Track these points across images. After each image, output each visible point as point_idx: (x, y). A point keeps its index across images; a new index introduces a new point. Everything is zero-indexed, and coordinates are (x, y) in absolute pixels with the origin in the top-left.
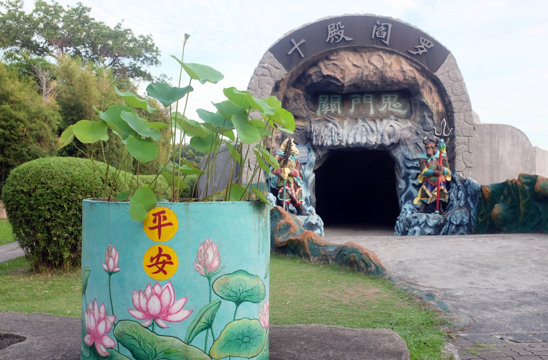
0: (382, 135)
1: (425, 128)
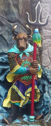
1: (10, 18)
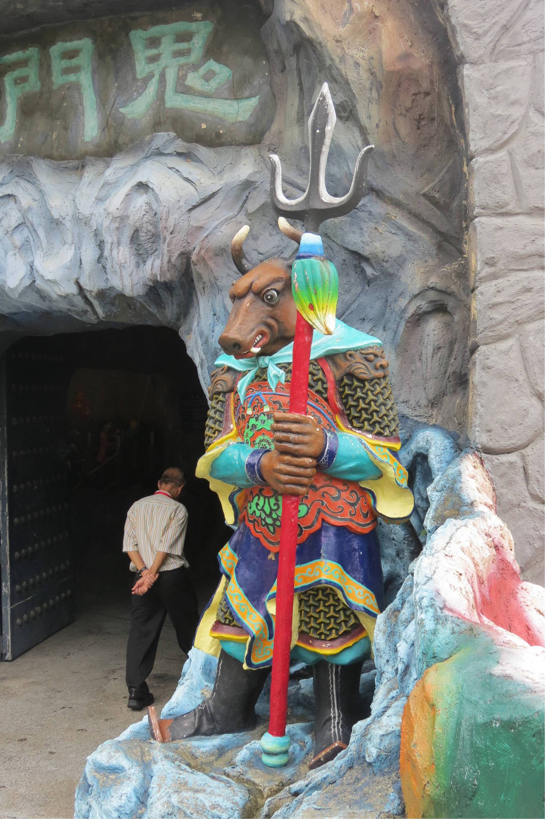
0: (101, 245)
